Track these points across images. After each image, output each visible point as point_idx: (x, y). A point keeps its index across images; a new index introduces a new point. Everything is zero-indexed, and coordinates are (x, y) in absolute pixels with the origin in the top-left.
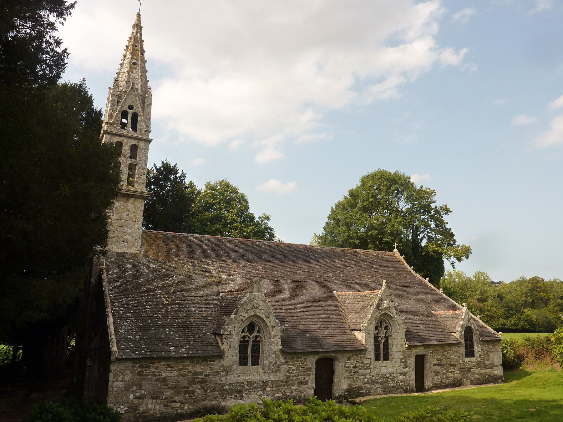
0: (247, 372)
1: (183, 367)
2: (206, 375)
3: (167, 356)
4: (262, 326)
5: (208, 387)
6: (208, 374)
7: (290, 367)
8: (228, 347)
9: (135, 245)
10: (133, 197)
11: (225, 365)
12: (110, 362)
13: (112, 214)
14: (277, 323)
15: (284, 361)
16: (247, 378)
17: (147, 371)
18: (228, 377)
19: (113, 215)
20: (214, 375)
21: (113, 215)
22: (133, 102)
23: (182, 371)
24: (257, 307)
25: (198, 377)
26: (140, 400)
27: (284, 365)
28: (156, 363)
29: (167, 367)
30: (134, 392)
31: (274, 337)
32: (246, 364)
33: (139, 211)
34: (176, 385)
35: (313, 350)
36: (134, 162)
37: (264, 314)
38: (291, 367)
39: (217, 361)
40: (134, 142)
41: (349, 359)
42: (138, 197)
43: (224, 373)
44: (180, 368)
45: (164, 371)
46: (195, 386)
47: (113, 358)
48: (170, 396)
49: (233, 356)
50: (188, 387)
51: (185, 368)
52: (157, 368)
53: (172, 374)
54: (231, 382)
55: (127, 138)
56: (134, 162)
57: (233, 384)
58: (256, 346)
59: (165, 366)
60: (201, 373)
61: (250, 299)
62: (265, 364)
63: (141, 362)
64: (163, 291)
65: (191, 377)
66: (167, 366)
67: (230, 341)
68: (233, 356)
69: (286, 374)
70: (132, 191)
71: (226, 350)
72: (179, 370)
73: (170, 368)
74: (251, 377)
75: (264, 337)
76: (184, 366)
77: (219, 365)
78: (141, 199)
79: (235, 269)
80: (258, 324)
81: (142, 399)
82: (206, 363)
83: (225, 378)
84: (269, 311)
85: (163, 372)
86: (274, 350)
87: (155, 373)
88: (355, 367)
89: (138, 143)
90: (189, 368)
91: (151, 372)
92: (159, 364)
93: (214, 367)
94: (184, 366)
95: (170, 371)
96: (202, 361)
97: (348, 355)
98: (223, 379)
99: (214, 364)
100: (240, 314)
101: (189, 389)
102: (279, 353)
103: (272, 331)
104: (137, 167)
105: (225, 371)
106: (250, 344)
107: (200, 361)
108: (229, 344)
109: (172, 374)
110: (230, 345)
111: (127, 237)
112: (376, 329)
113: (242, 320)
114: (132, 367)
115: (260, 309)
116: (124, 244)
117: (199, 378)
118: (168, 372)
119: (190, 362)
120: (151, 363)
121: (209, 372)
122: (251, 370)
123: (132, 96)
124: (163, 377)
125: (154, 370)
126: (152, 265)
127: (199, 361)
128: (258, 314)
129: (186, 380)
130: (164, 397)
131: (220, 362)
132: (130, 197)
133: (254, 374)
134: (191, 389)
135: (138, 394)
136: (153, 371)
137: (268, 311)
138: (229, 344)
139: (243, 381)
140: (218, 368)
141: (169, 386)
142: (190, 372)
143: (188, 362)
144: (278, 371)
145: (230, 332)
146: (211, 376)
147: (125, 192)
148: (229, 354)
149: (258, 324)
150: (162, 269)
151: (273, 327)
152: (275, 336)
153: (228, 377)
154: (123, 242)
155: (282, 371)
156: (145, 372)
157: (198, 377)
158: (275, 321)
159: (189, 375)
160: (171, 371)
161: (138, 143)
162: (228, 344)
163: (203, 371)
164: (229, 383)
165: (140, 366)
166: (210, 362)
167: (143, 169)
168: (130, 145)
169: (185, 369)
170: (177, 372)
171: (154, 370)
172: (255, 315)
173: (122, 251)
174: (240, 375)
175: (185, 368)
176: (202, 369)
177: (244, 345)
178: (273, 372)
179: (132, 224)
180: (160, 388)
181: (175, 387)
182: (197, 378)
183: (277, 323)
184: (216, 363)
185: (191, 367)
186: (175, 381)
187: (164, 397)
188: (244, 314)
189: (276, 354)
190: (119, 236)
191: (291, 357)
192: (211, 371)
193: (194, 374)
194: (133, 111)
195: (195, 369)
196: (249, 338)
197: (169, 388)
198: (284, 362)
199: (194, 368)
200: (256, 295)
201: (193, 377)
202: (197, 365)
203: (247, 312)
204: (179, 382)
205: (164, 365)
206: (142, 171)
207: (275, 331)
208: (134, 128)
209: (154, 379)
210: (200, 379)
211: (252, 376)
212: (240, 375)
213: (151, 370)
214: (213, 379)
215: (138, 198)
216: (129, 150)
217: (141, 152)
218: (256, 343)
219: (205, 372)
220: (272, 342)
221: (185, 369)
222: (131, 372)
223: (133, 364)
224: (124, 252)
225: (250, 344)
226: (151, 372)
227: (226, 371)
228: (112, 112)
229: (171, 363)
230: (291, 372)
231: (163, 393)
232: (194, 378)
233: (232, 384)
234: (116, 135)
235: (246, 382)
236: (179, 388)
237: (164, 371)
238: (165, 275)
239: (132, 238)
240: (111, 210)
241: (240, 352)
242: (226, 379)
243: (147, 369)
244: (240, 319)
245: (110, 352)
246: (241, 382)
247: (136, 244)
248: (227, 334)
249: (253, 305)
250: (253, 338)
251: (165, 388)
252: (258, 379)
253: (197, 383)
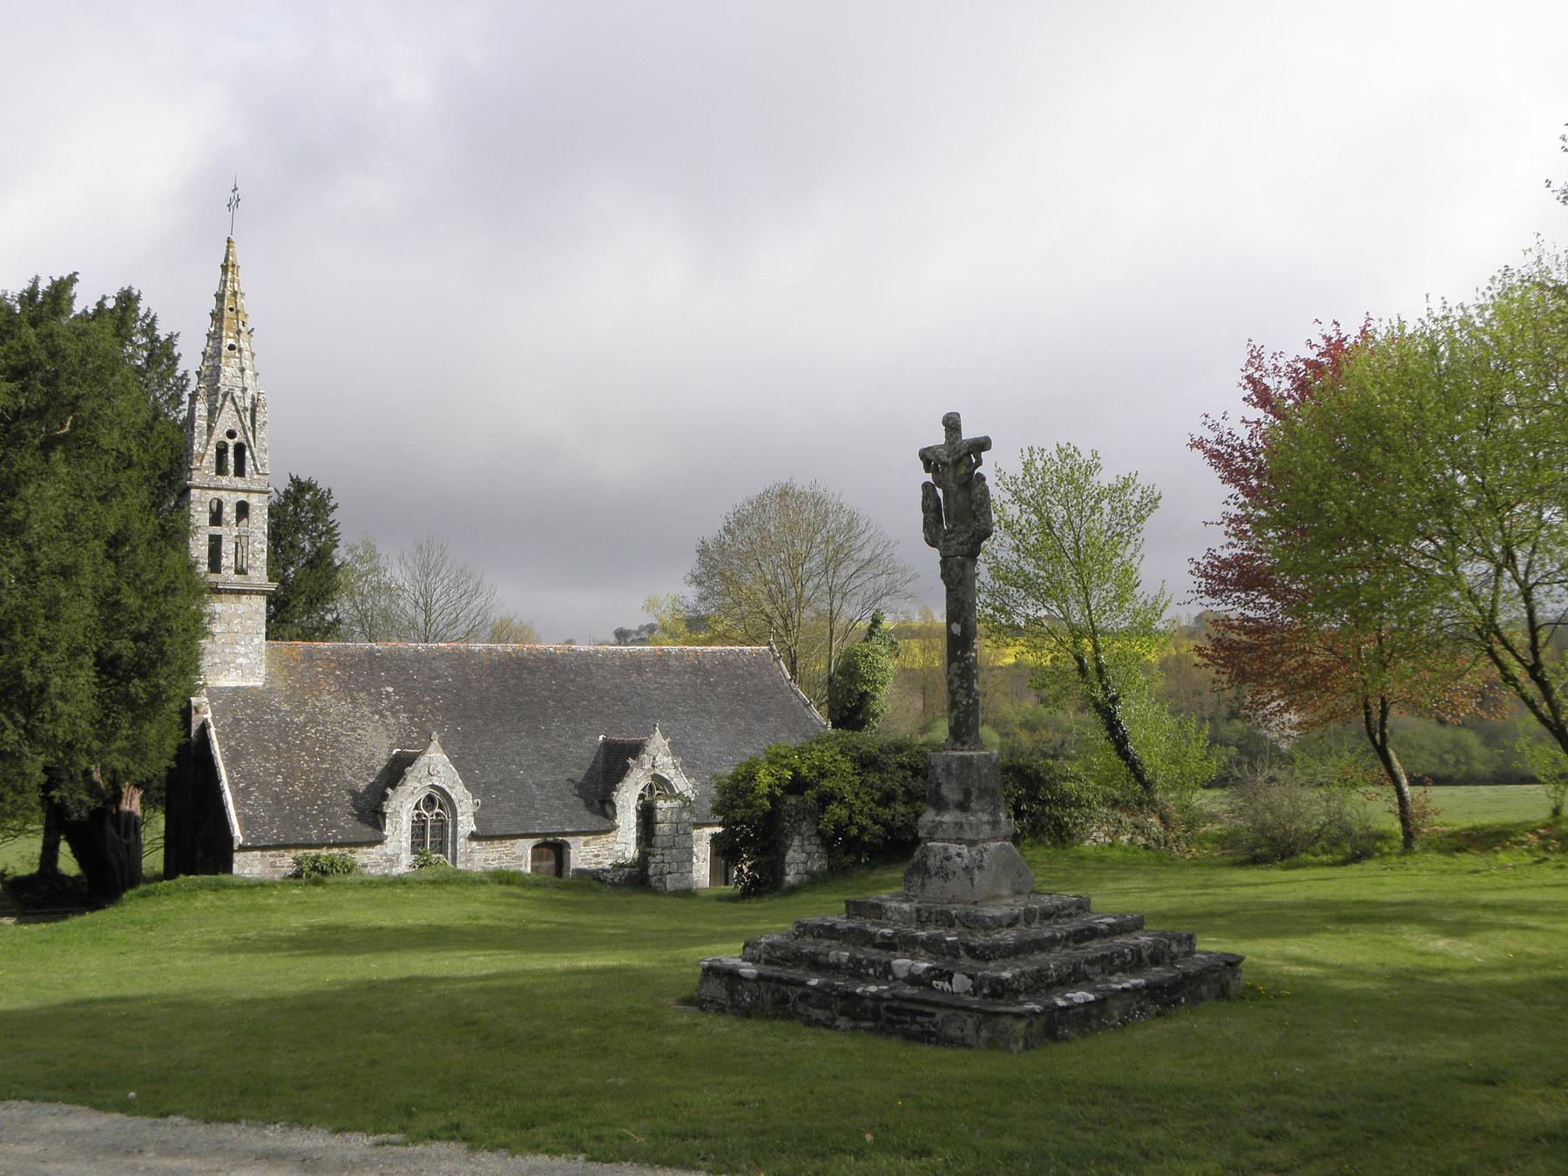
3: (306, 842)
10: (245, 594)
12: (233, 851)
35: (523, 832)
40: (242, 497)
41: (586, 844)
47: (236, 846)
58: (441, 827)
64: (302, 751)
79: (425, 704)
88: (597, 856)
93: (372, 856)
97: (584, 838)
111: (241, 660)
112: (639, 799)
126: (286, 707)
128: (437, 784)
150: (301, 713)
167: (260, 543)
168: (236, 502)
172: (432, 786)
173: (234, 684)
179: (248, 638)
190: (228, 660)
194: (236, 440)
203: (419, 782)
206: (259, 546)
207: (464, 807)
208: (240, 472)
222: (260, 863)
224: (238, 687)
234: (209, 488)
238: (305, 725)
241: (413, 835)
244: (409, 791)
245: (230, 839)
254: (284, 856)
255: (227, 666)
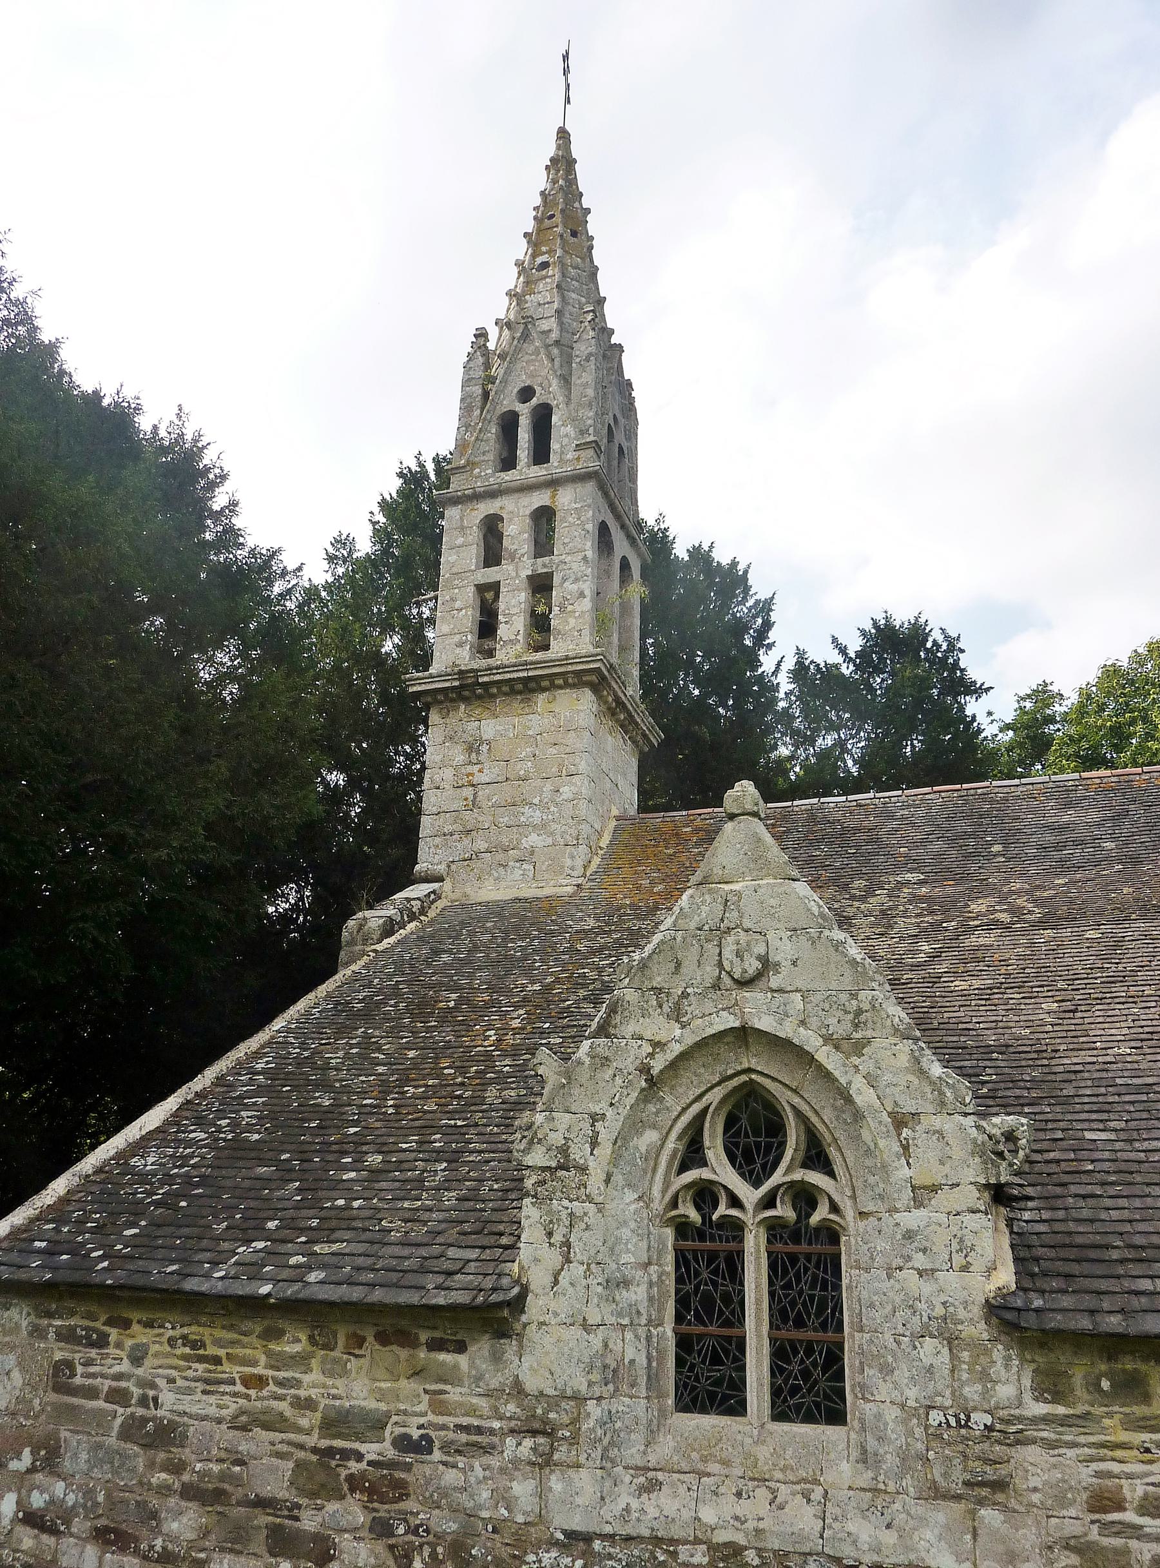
0: (726, 1463)
1: (272, 1367)
2: (404, 1443)
4: (827, 1119)
5: (415, 1532)
6: (416, 1434)
7: (1115, 1467)
8: (553, 1258)
9: (563, 867)
11: (531, 1384)
13: (476, 768)
14: (937, 1086)
15: (1041, 1409)
16: (708, 1515)
17: (92, 1369)
18: (556, 1483)
19: (480, 771)
20: (458, 1452)
21: (480, 771)
22: (532, 376)
23: (265, 1393)
24: (751, 971)
25: (356, 1445)
26: (45, 1538)
27: (1051, 1445)
28: (136, 1328)
29: (185, 1357)
30: (22, 1480)
31: (922, 1194)
32: (737, 1408)
33: (572, 734)
34: (223, 1477)
36: (544, 566)
37: (814, 1022)
38: (1130, 1476)
39: (481, 1347)
40: (540, 499)
42: (561, 682)
43: (528, 1443)
44: (255, 1371)
45: (171, 1381)
46: (332, 1507)
48: (192, 1545)
49: (586, 1327)
50: (290, 1510)
51: (282, 1374)
52: (137, 1359)
53: (209, 1405)
54: (577, 1523)
55: (516, 495)
56: (544, 566)
57: (597, 1545)
59: (178, 1352)
60: (376, 1425)
61: (693, 925)
62: (879, 1416)
63: (72, 1313)
65: (312, 1440)
66: (187, 1350)
67: (564, 1214)
68: (586, 1327)
69: (1075, 1528)
70: (530, 664)
71: (538, 1278)
72: (247, 1381)
73: (201, 1367)
74: (743, 1508)
75: (854, 1197)
76: (278, 1361)
77: (494, 1383)
78: (573, 686)
80: (796, 1100)
81: (54, 1531)
82: (403, 1353)
83: (530, 1485)
84: (854, 996)
85: (161, 1383)
86: (932, 1307)
87: (123, 1384)
89: (553, 497)
90: (306, 1379)
91: (103, 1376)
92: (148, 1330)
93: (454, 1394)
94: (278, 1361)
95: (200, 1386)
96: (383, 1339)
98: (522, 1489)
99: (456, 1366)
100: (630, 1029)
101: (297, 1519)
102: (979, 1330)
103: (896, 1148)
104: (556, 580)
105: (534, 1433)
106: (754, 1246)
107: (370, 1339)
108: (557, 1238)
109: (209, 1405)
110: (567, 1244)
111: (533, 839)
113: (645, 1069)
114: (30, 1334)
115: (780, 991)
116: (525, 870)
117: (359, 1457)
118: (189, 1391)
119: (311, 1338)
120: (110, 1322)
121: (422, 1420)
122: (763, 1453)
123: (527, 358)
124: (160, 1413)
125: (125, 1366)
127: (360, 1342)
128: (765, 1023)
129: (280, 1455)
130: (158, 1548)
131: (497, 1358)
132: (533, 691)
133: (774, 1492)
134: (309, 1523)
135: (37, 1500)
136: (117, 1369)
137: (844, 997)
138: (557, 1238)
139: (677, 1532)
140: (483, 1403)
141: (186, 1477)
142: (308, 1404)
143: (299, 1341)
144: (985, 1492)
145: (564, 1150)
146: (437, 1455)
147: (508, 676)
148: (563, 1306)
149: (796, 1100)
151: (900, 1121)
152: (934, 1189)
153: (556, 1483)
154: (518, 864)
155: (1036, 1498)
156: (80, 1369)
157: (356, 1445)
158: (922, 1073)
159: (304, 1422)
160: (207, 1381)
161: (553, 497)
162: (550, 1234)
163: (383, 1406)
164: (564, 1532)
165: (67, 1336)
166: (433, 1355)
168: (528, 512)
169: (280, 1383)
170: (235, 1395)
171: (125, 1366)
174: (660, 1476)
175: (282, 1374)
176: (381, 1396)
177: (712, 1256)
178: (936, 1494)
179: (548, 787)
180: (141, 1483)
181: (219, 1496)
182: (346, 1454)
183: (937, 1086)
184: (472, 1365)
185: (315, 1376)
186: (223, 1455)
187: (159, 1543)
188: (658, 1026)
189: (952, 1341)
191: (1105, 1375)
192: (441, 1420)
193: (334, 1423)
194: (534, 401)
195: (340, 1386)
196: (735, 1202)
197: (189, 1493)
198: (1046, 1419)
199: (330, 1382)
200: (738, 894)
201: (324, 1443)
202: (353, 1363)
203: (677, 1015)
204: (240, 1462)
205: (171, 1341)
206: (574, 587)
207: (926, 1153)
208: (541, 454)
209: (119, 1421)
210: (363, 1465)
211: (757, 1505)
212: (660, 1476)
213: (110, 1361)
214: (451, 1477)
215: (560, 687)
216: (524, 533)
217: (565, 524)
218: (804, 1247)
219: (395, 1418)
220: (909, 1235)
221: (280, 1383)
223: (39, 1316)
225: (754, 1246)
226: (103, 1376)
227: (543, 1430)
228: (467, 431)
229: (206, 1331)
230: (1130, 1516)
231: (154, 1515)
232: (330, 1452)
233: (588, 1538)
235: (697, 1541)
236: (239, 1504)
237: (171, 1381)
239: (550, 841)
240: (474, 754)
242: (542, 1493)
243: (93, 1353)
244: (629, 1063)
246: (657, 1541)
247: (569, 862)
248: (544, 1169)
249: (720, 964)
250: (769, 1202)
251: (164, 1490)
252: (800, 1537)
253: (346, 1487)
254: (101, 1342)
255: (500, 857)
